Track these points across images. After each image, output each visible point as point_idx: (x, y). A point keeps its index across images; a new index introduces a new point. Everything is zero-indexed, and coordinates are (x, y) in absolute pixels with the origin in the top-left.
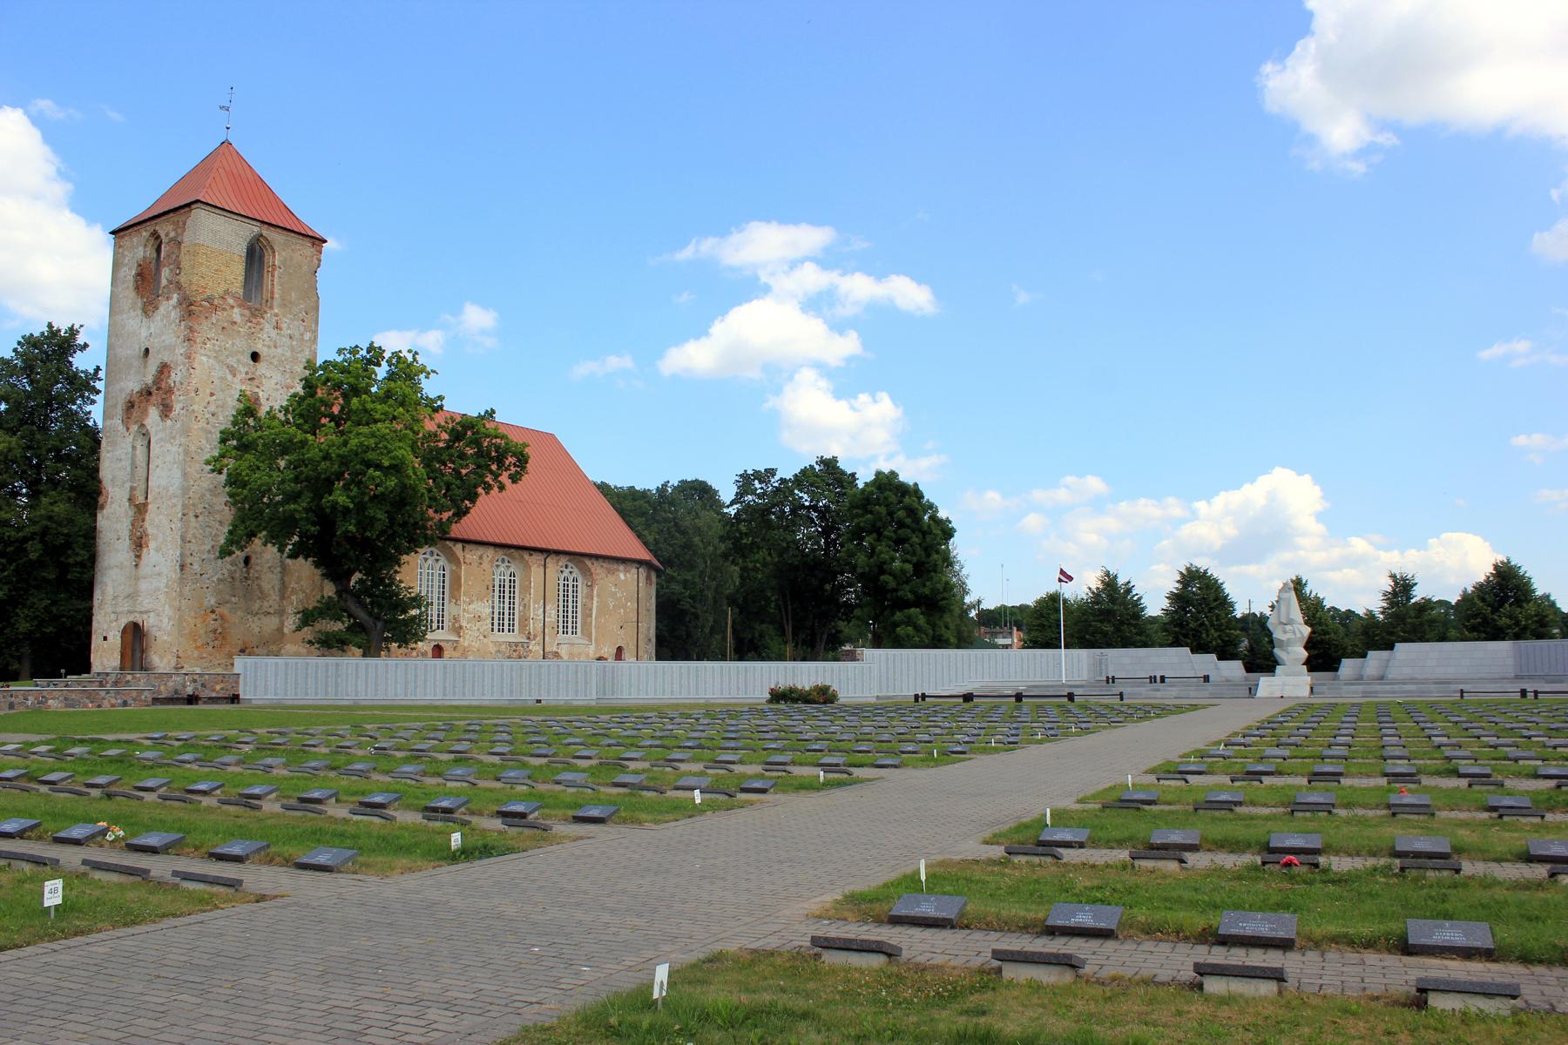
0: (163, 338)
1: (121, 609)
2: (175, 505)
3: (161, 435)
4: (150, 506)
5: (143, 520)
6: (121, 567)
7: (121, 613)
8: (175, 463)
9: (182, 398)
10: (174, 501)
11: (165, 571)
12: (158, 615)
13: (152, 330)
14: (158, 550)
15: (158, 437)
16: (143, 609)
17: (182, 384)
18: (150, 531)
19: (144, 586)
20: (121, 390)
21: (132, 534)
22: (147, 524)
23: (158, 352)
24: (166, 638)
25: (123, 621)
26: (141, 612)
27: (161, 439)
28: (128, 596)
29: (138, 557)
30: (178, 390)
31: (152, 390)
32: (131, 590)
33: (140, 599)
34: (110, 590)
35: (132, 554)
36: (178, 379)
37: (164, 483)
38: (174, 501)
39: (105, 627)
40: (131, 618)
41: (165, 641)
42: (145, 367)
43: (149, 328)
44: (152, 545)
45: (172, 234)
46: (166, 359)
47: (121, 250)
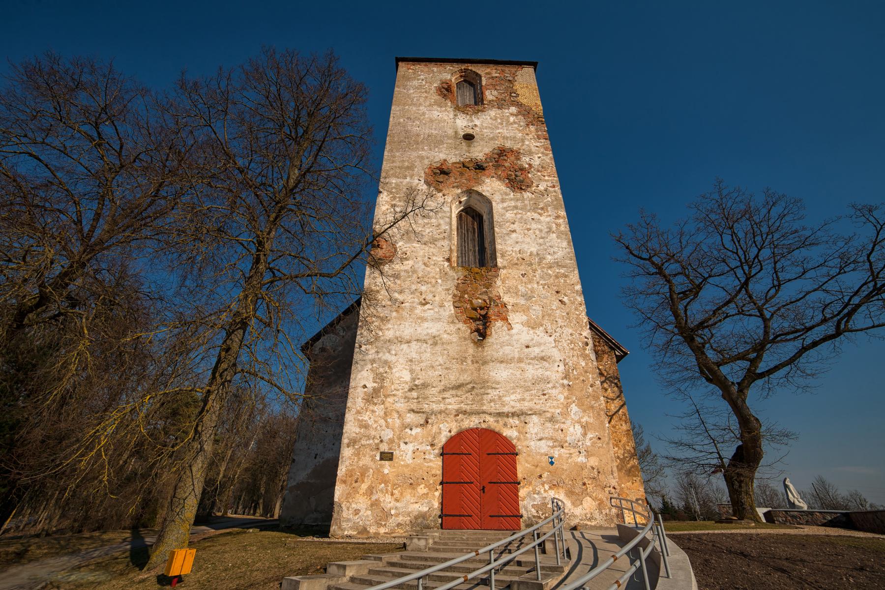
0: (498, 131)
1: (435, 407)
2: (566, 276)
3: (513, 203)
4: (503, 272)
5: (489, 286)
6: (435, 341)
7: (433, 413)
8: (550, 231)
9: (546, 178)
10: (562, 271)
11: (556, 354)
12: (552, 420)
13: (477, 122)
14: (532, 325)
15: (505, 205)
16: (506, 409)
17: (542, 167)
18: (506, 299)
19: (500, 373)
20: (422, 158)
21: (458, 301)
22: (500, 288)
23: (492, 139)
24: (581, 459)
25: (445, 430)
26: (500, 414)
27: (516, 207)
28: (458, 387)
29: (482, 333)
30: (538, 171)
31: (485, 165)
32: (465, 378)
33: (493, 394)
34: (401, 374)
35: (465, 329)
36: (536, 162)
37: (534, 250)
38: (562, 271)
39: (388, 434)
40: (472, 422)
41: (582, 467)
42: (469, 146)
43: (472, 121)
44: (516, 318)
45: (497, 75)
46: (508, 144)
47: (410, 71)
